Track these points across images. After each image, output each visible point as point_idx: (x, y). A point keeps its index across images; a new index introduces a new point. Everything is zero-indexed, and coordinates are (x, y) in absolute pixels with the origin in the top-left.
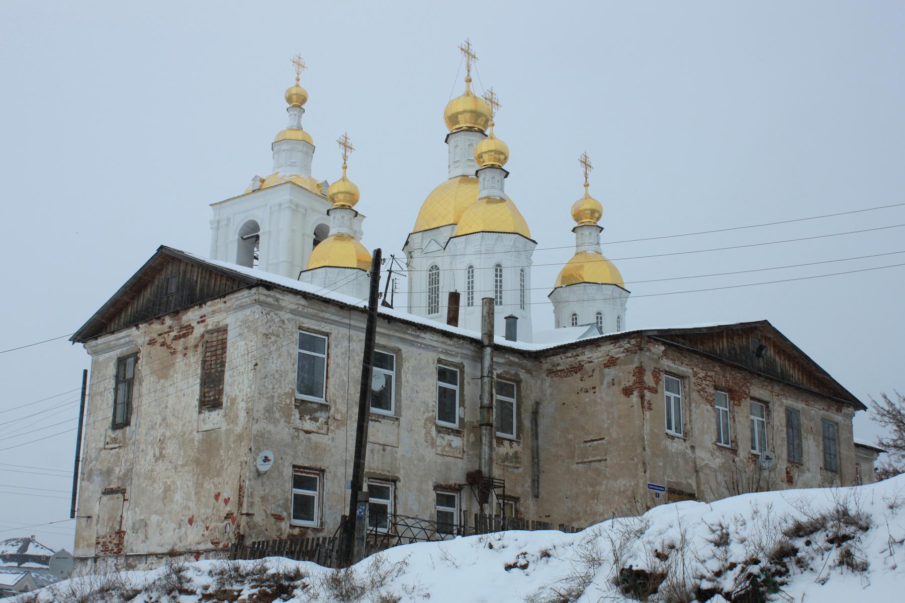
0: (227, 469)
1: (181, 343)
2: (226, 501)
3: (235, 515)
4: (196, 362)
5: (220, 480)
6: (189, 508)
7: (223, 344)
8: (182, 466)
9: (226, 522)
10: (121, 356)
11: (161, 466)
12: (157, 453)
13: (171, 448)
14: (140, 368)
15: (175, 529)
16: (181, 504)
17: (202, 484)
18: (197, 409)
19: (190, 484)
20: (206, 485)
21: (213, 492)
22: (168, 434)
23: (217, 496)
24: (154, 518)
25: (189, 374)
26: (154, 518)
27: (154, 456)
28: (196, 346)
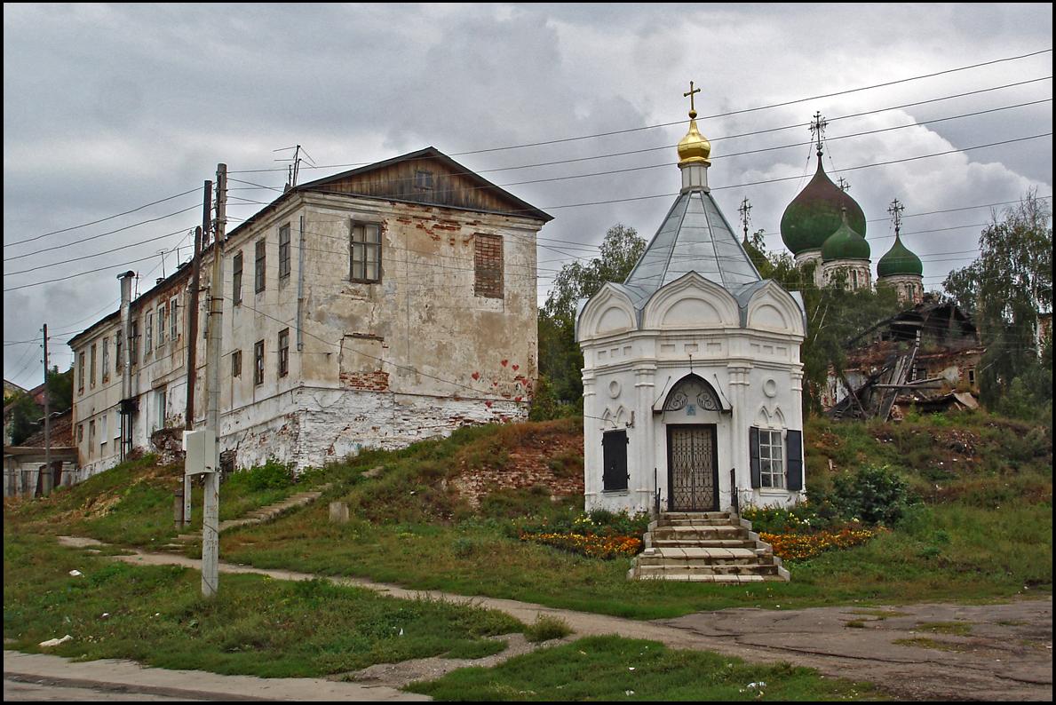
0: (513, 344)
2: (515, 368)
3: (526, 378)
4: (468, 254)
5: (507, 351)
6: (471, 367)
7: (497, 251)
8: (459, 333)
9: (516, 383)
11: (429, 327)
12: (424, 316)
13: (442, 316)
14: (389, 238)
17: (486, 351)
18: (473, 292)
19: (472, 348)
20: (490, 352)
21: (500, 358)
22: (437, 304)
23: (505, 363)
27: (421, 317)
28: (466, 242)
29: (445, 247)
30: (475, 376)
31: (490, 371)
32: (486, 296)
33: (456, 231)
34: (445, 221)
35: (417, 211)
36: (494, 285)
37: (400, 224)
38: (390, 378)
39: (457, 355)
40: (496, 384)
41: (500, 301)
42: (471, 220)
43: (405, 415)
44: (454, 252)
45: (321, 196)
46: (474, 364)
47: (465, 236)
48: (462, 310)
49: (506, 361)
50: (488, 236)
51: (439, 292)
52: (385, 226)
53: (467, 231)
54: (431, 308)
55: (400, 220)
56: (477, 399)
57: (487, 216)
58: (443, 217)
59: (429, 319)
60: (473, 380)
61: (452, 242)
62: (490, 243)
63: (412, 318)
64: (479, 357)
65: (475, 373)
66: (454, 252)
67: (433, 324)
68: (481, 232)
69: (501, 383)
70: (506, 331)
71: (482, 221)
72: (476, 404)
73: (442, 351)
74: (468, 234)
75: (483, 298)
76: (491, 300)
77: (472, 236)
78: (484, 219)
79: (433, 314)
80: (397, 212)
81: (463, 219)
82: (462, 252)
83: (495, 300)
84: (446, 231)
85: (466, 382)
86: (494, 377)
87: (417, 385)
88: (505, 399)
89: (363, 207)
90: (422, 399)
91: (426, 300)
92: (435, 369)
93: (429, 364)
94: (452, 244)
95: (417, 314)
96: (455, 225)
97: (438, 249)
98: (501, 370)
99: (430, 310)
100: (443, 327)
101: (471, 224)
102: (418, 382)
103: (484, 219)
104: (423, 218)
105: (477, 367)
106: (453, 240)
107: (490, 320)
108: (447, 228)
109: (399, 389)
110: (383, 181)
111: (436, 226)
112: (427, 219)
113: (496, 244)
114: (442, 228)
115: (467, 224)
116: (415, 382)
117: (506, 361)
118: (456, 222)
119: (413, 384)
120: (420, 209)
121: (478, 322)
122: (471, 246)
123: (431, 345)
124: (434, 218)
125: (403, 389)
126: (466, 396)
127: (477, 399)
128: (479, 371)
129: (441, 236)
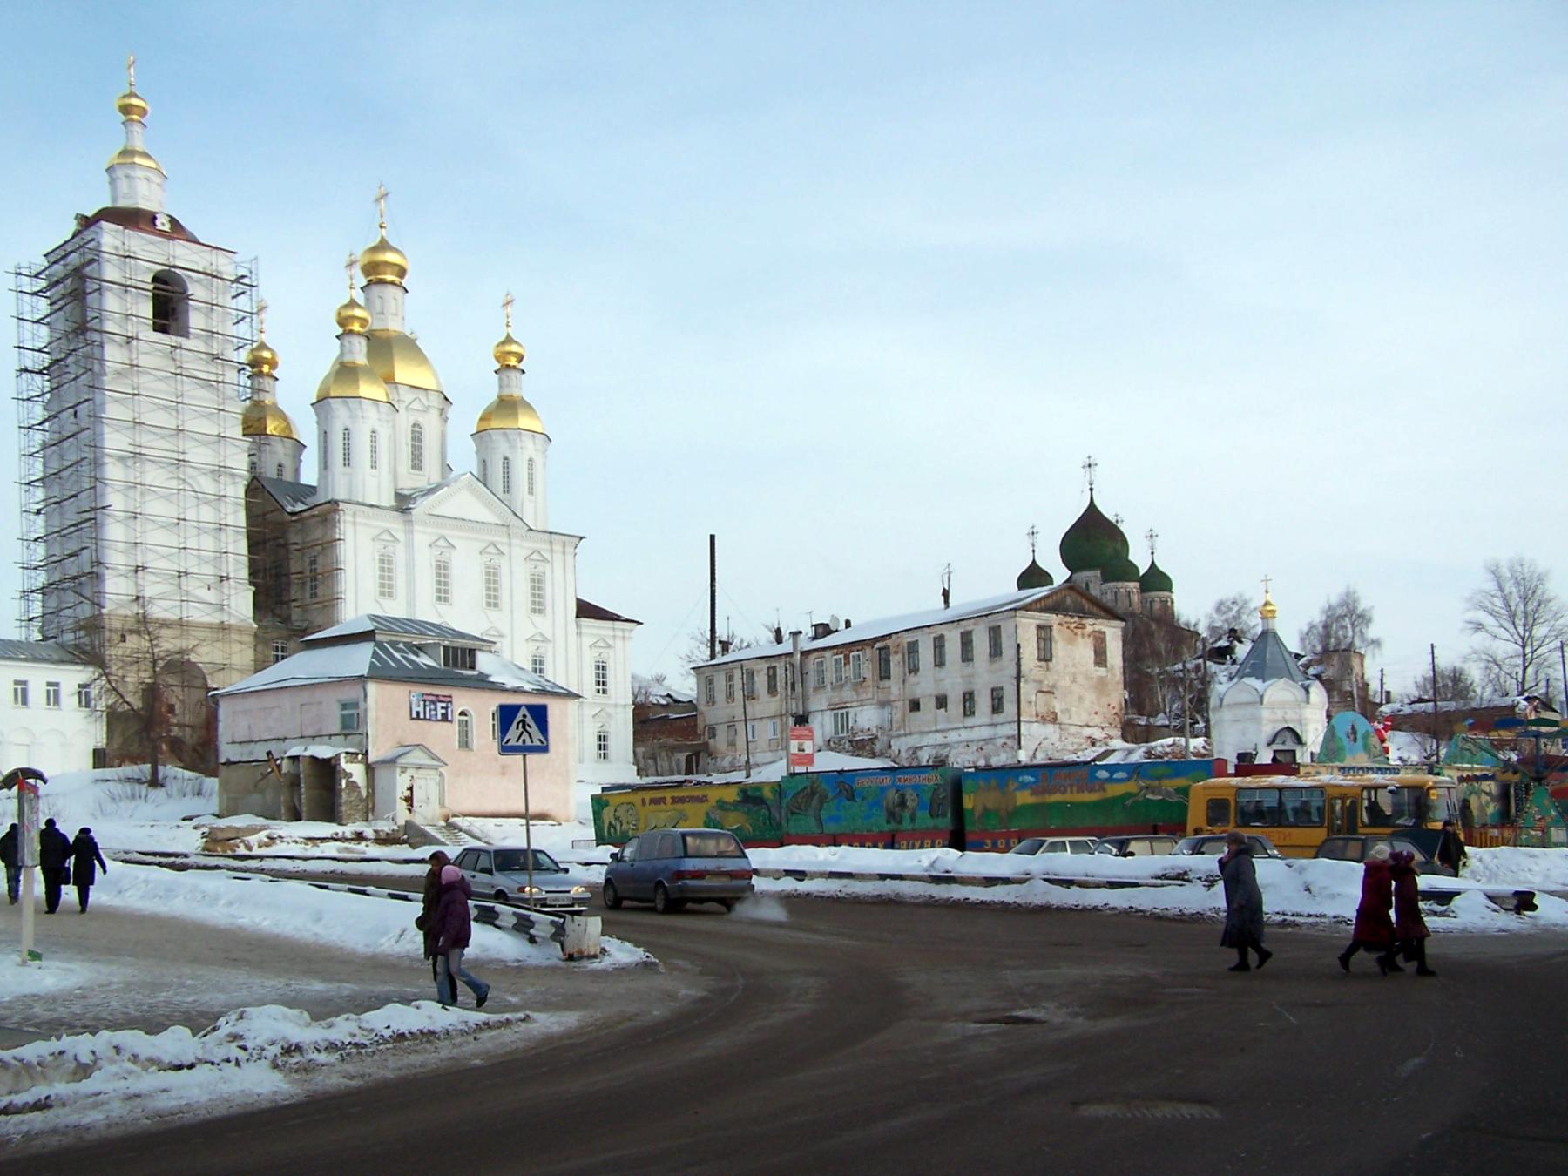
13: (1080, 679)
24: (1074, 709)
26: (1074, 709)
29: (1080, 639)
30: (1096, 713)
39: (1087, 703)
53: (1089, 629)
91: (1073, 670)
102: (1070, 717)
105: (1097, 709)
122: (1091, 638)
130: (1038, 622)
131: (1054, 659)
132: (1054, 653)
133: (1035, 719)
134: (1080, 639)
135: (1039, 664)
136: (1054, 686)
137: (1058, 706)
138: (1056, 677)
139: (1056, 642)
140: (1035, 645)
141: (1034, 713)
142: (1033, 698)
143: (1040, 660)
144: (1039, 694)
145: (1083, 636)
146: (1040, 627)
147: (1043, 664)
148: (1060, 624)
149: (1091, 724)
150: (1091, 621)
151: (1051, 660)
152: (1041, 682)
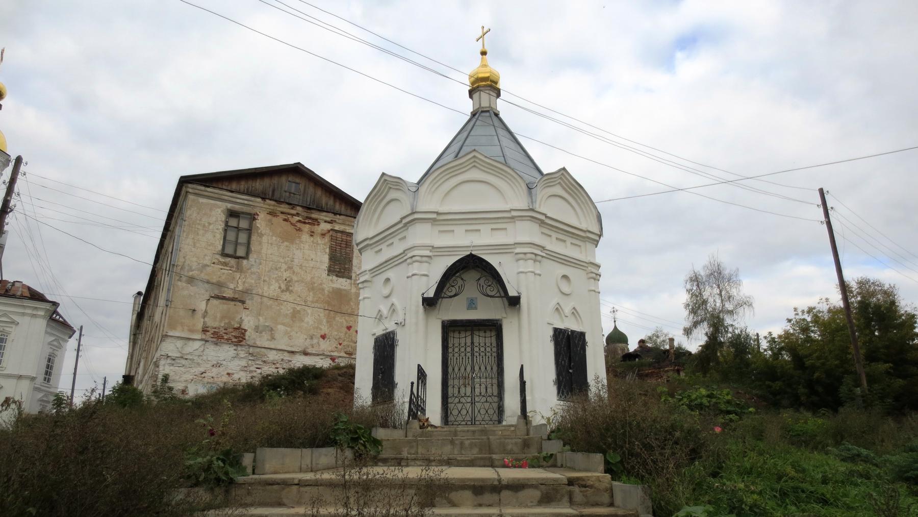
1: (307, 227)
4: (325, 244)
6: (321, 329)
10: (232, 209)
11: (286, 296)
12: (283, 287)
13: (297, 288)
15: (306, 339)
16: (312, 325)
17: (334, 318)
18: (327, 272)
21: (345, 324)
22: (295, 278)
24: (280, 327)
25: (317, 249)
27: (280, 288)
28: (323, 235)
29: (305, 237)
30: (323, 337)
31: (336, 333)
32: (337, 276)
33: (316, 226)
34: (307, 218)
35: (284, 208)
36: (345, 269)
37: (269, 217)
38: (247, 334)
39: (309, 320)
40: (340, 344)
41: (348, 280)
42: (328, 219)
43: (258, 364)
44: (313, 241)
45: (203, 188)
46: (323, 327)
47: (322, 230)
48: (316, 285)
49: (351, 327)
50: (342, 232)
51: (297, 269)
52: (256, 217)
53: (325, 227)
54: (289, 281)
55: (270, 213)
56: (323, 355)
57: (342, 217)
58: (305, 214)
59: (287, 289)
60: (321, 339)
61: (312, 234)
62: (343, 237)
63: (272, 287)
64: (328, 322)
65: (323, 334)
66: (313, 241)
67: (290, 293)
68: (336, 229)
69: (345, 343)
70: (352, 304)
71: (337, 220)
72: (322, 359)
73: (295, 315)
74: (325, 229)
75: (335, 278)
76: (341, 280)
77: (329, 231)
78: (339, 219)
79: (291, 286)
80: (268, 207)
81: (322, 217)
82: (320, 242)
83: (345, 279)
84: (308, 225)
85: (315, 341)
86: (340, 338)
87: (271, 341)
88: (347, 356)
89: (238, 201)
90: (274, 352)
91: (286, 275)
92: (289, 329)
93: (283, 324)
94: (311, 236)
95: (277, 285)
96: (316, 222)
97: (300, 237)
98: (346, 333)
99: (289, 282)
100: (299, 296)
101: (329, 222)
102: (273, 338)
103: (339, 219)
104: (289, 214)
105: (325, 330)
106: (313, 232)
107: (339, 295)
108: (309, 223)
109: (255, 343)
110: (258, 185)
111: (299, 221)
112: (293, 215)
113: (348, 239)
114: (305, 223)
115: (325, 222)
116: (269, 338)
117: (351, 327)
118: (316, 220)
119: (268, 340)
120: (287, 206)
121: (328, 295)
122: (327, 239)
123: (287, 309)
124: (298, 214)
125: (259, 343)
126: (314, 352)
127: (323, 355)
128: (327, 333)
129: (303, 229)
130: (229, 206)
131: (252, 257)
132: (253, 247)
133: (198, 336)
134: (305, 237)
135: (222, 260)
136: (246, 292)
137: (248, 322)
138: (251, 281)
139: (261, 235)
140: (219, 236)
141: (200, 326)
142: (202, 306)
143: (224, 254)
144: (215, 302)
145: (312, 234)
146: (232, 214)
147: (232, 262)
148: (272, 214)
149: (309, 351)
150: (329, 217)
151: (246, 257)
152: (220, 285)
